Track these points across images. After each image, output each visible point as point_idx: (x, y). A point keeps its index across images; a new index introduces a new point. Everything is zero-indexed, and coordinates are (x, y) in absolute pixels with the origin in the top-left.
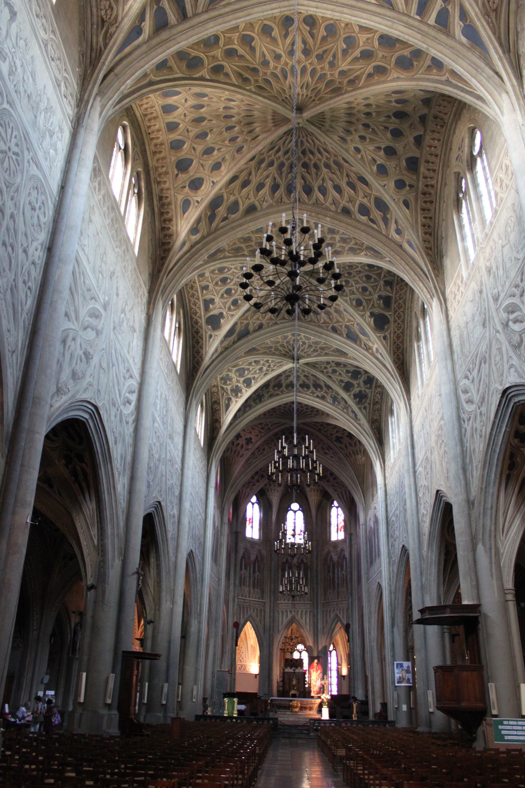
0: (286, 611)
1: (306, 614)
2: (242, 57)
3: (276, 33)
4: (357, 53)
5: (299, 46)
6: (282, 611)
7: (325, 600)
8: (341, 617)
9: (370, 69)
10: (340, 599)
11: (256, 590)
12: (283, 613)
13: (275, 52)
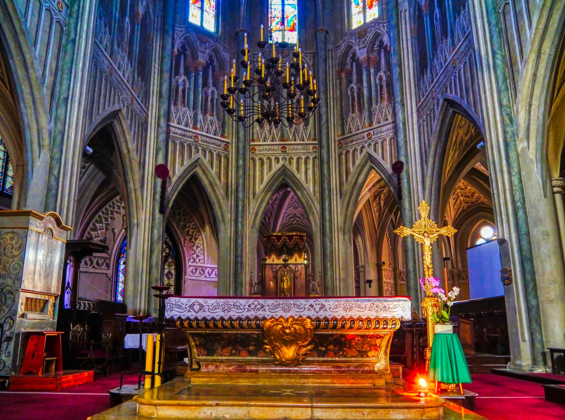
0: (269, 158)
1: (306, 163)
6: (261, 160)
7: (343, 134)
8: (378, 157)
10: (375, 125)
11: (209, 118)
12: (262, 164)
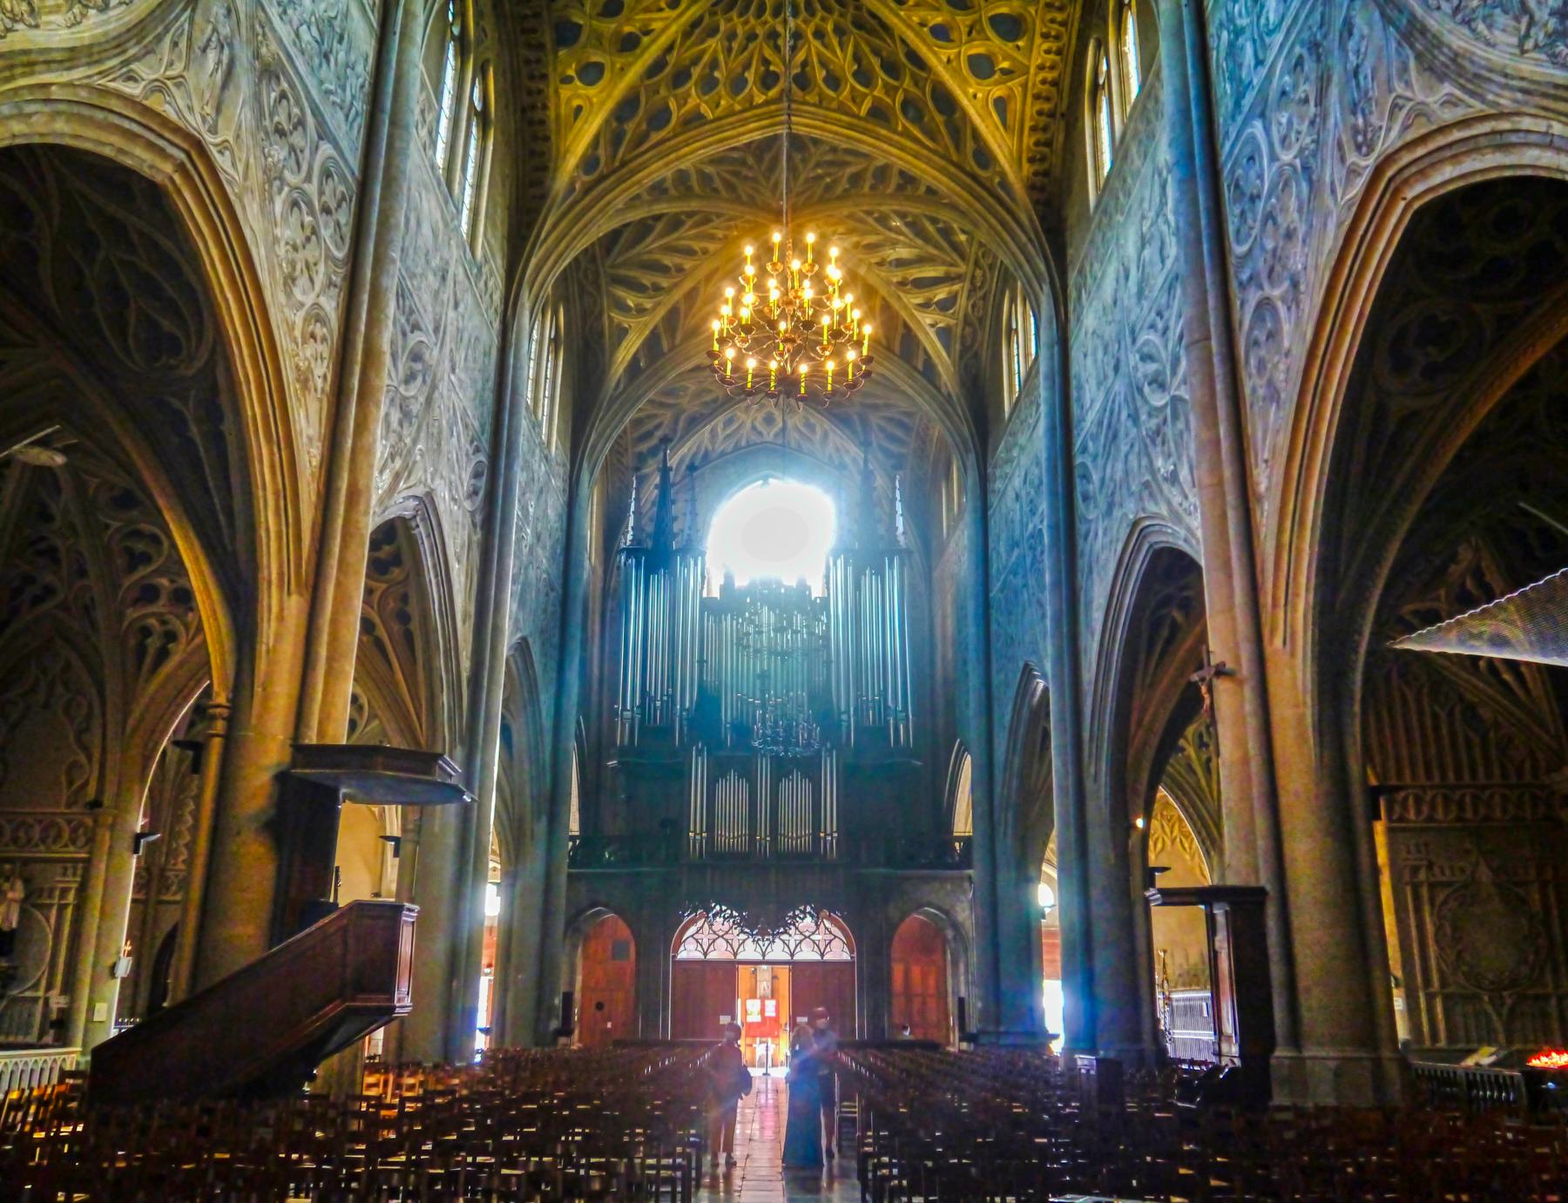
2: (876, 52)
3: (820, 74)
4: (696, 72)
5: (786, 42)
9: (672, 59)
13: (825, 46)
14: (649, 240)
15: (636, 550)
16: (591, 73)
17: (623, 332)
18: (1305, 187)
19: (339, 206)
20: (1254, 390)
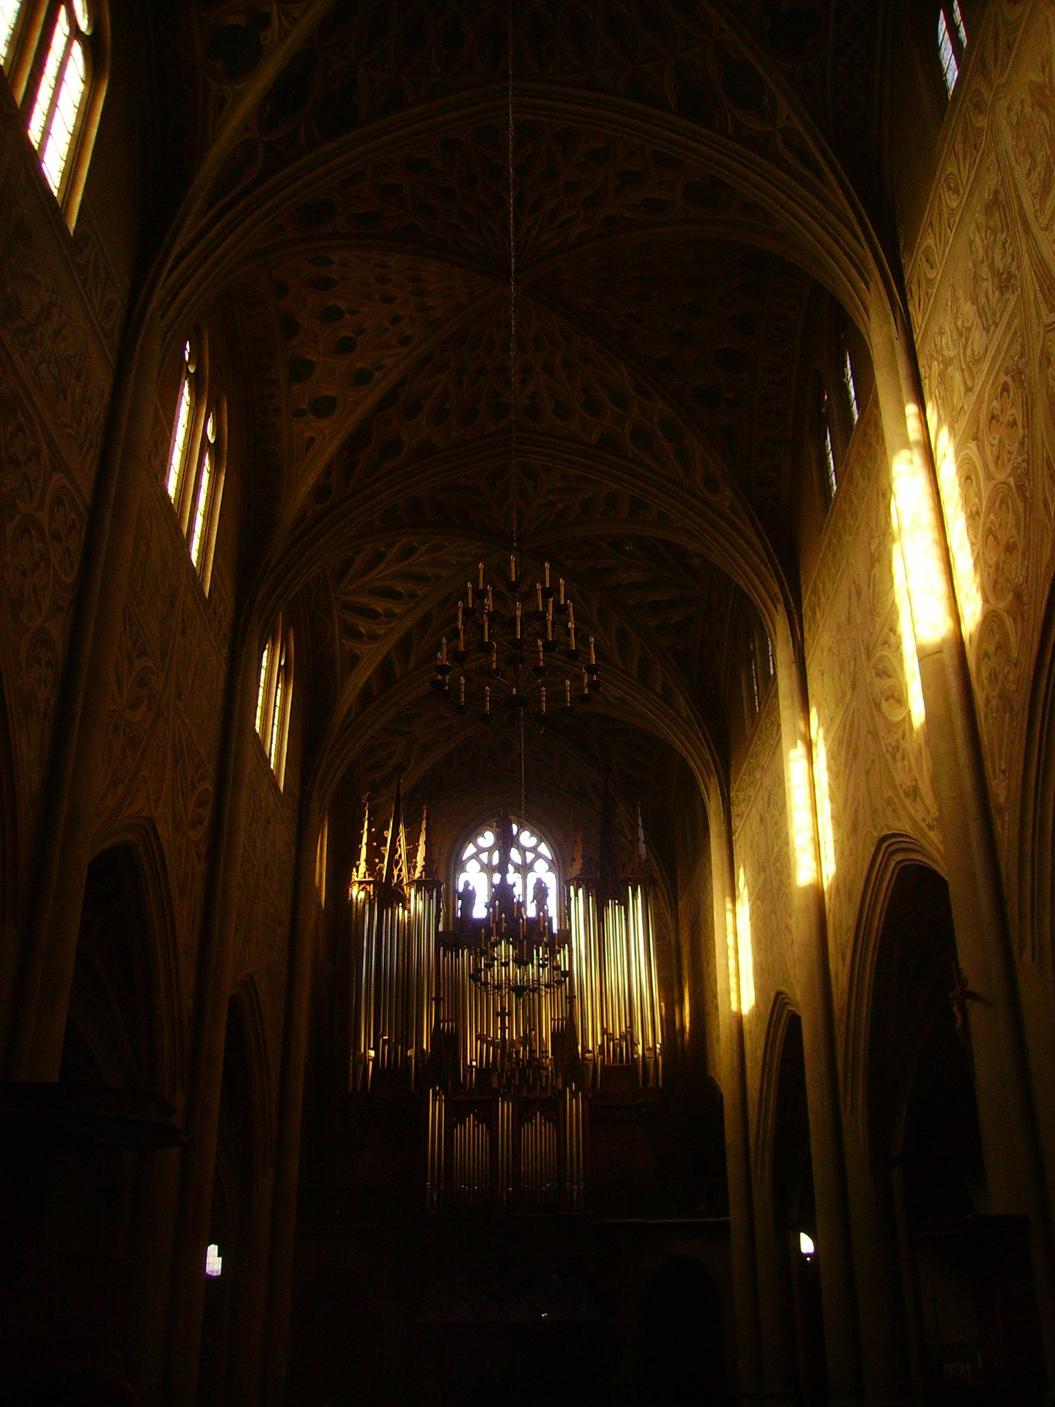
14: (382, 566)
15: (368, 883)
16: (323, 407)
17: (354, 660)
18: (1020, 505)
19: (69, 533)
20: (988, 701)
